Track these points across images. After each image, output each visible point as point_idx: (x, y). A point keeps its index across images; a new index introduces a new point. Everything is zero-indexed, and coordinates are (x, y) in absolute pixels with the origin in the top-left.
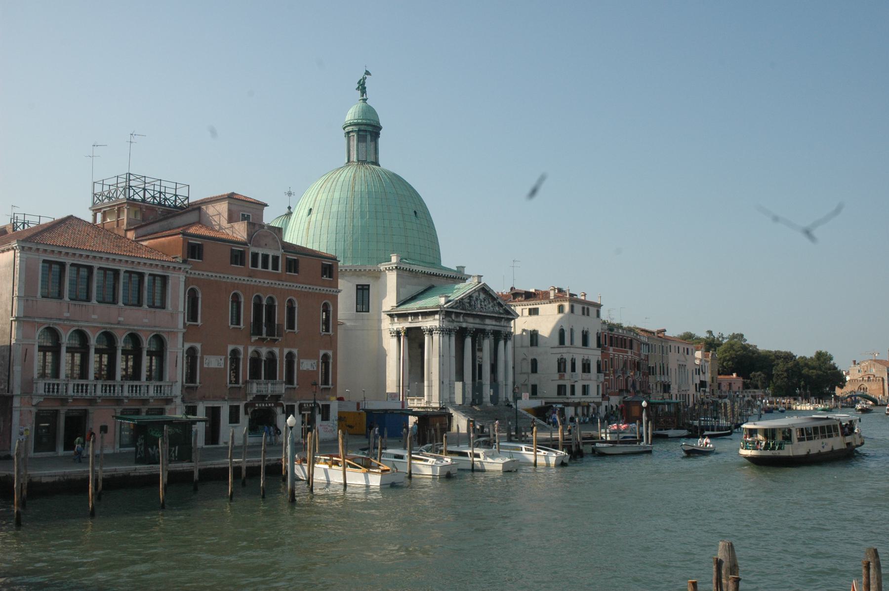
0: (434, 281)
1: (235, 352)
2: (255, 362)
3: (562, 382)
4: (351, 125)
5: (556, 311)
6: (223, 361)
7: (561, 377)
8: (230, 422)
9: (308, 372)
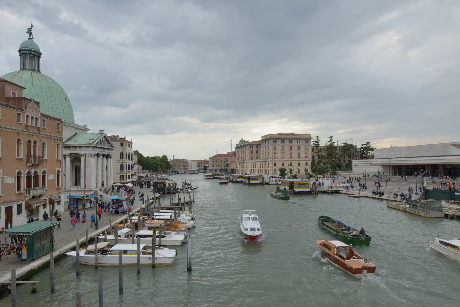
0: (77, 131)
1: (19, 173)
2: (29, 177)
3: (122, 174)
4: (25, 50)
5: (120, 145)
6: (13, 179)
7: (121, 173)
8: (18, 214)
9: (52, 180)
